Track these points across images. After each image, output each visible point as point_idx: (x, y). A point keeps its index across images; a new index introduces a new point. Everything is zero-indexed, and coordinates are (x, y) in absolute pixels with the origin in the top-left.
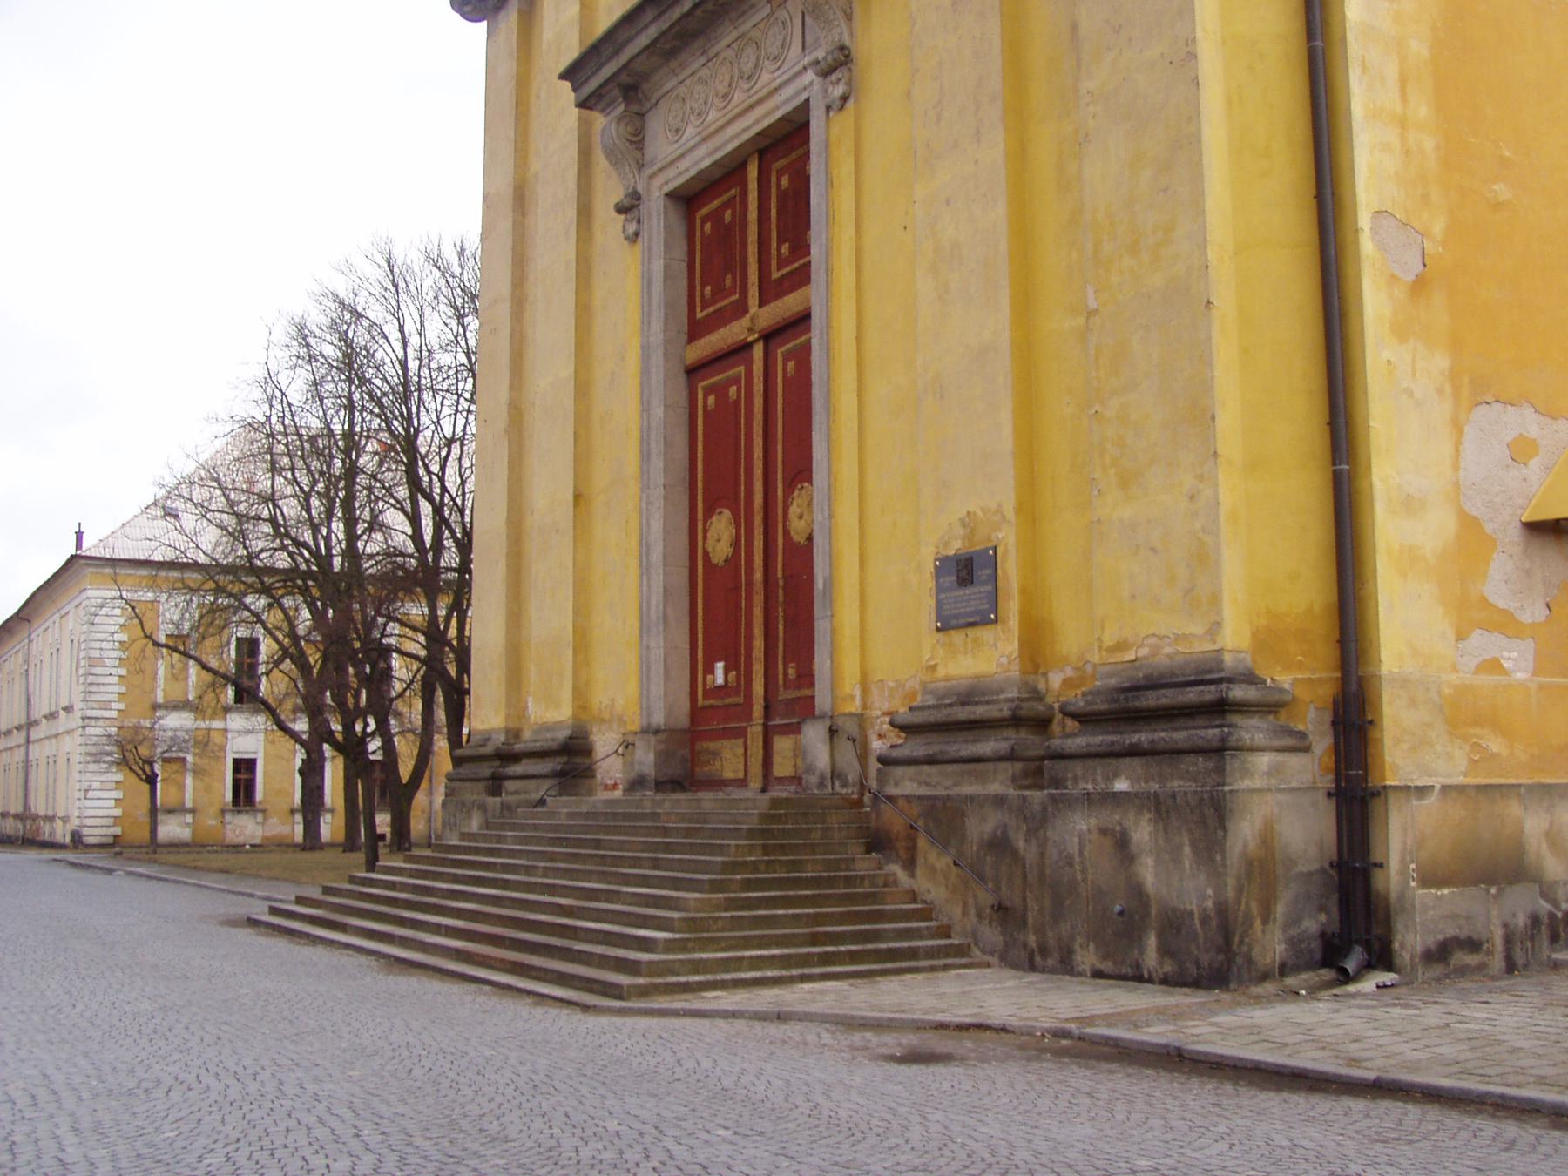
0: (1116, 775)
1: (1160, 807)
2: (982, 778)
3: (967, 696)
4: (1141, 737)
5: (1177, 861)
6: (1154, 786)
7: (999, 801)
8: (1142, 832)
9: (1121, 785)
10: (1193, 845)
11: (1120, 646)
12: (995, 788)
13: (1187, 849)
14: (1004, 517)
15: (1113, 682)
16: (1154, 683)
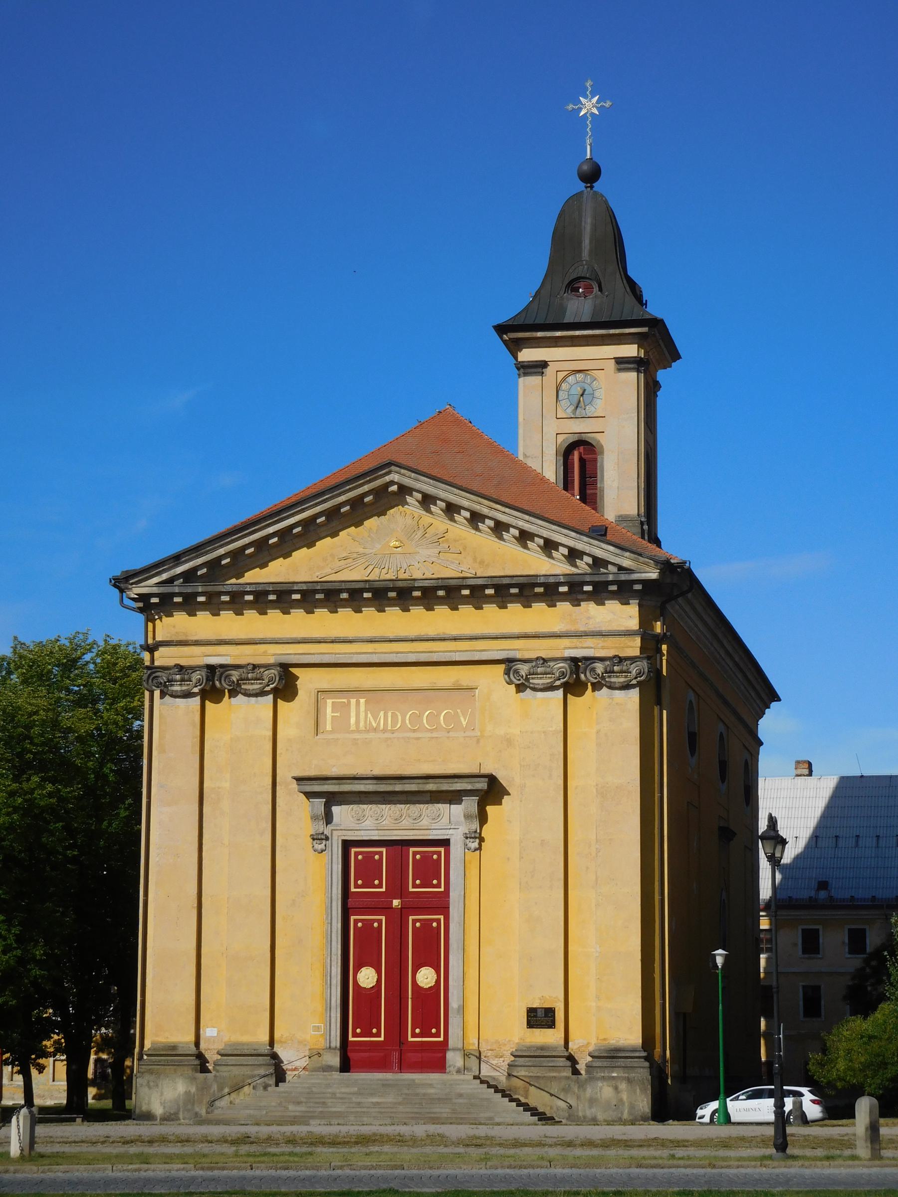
0: (613, 1072)
1: (629, 1081)
2: (559, 1072)
3: (542, 1048)
4: (621, 1062)
5: (635, 1092)
6: (627, 1075)
7: (568, 1078)
8: (623, 1086)
9: (615, 1075)
10: (640, 1089)
11: (605, 1039)
12: (564, 1074)
13: (638, 1090)
14: (559, 1000)
15: (603, 1048)
16: (618, 1050)
